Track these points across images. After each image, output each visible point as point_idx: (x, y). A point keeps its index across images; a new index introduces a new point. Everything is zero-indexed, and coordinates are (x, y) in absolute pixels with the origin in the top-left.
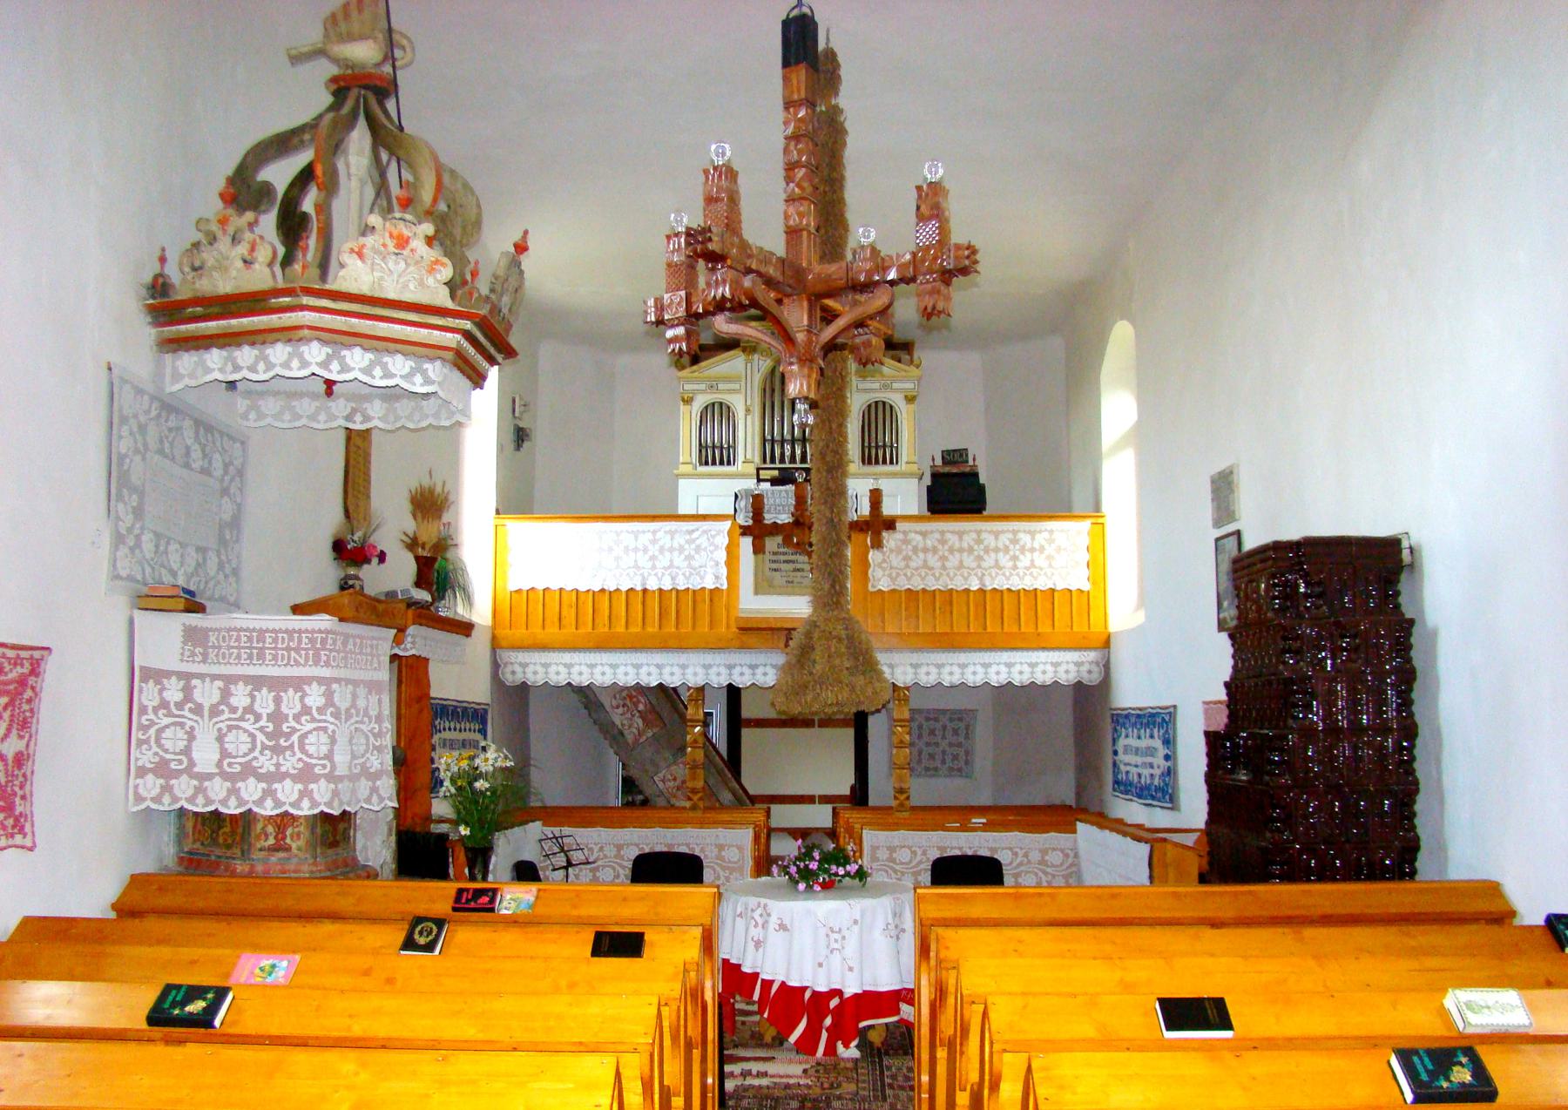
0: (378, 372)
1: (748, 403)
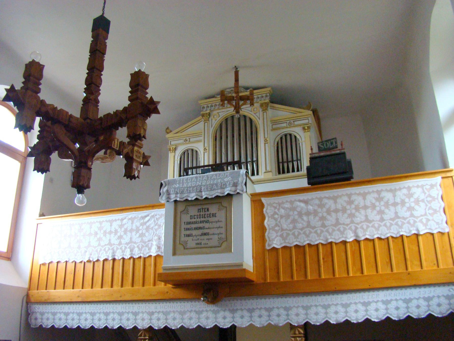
1: (206, 145)
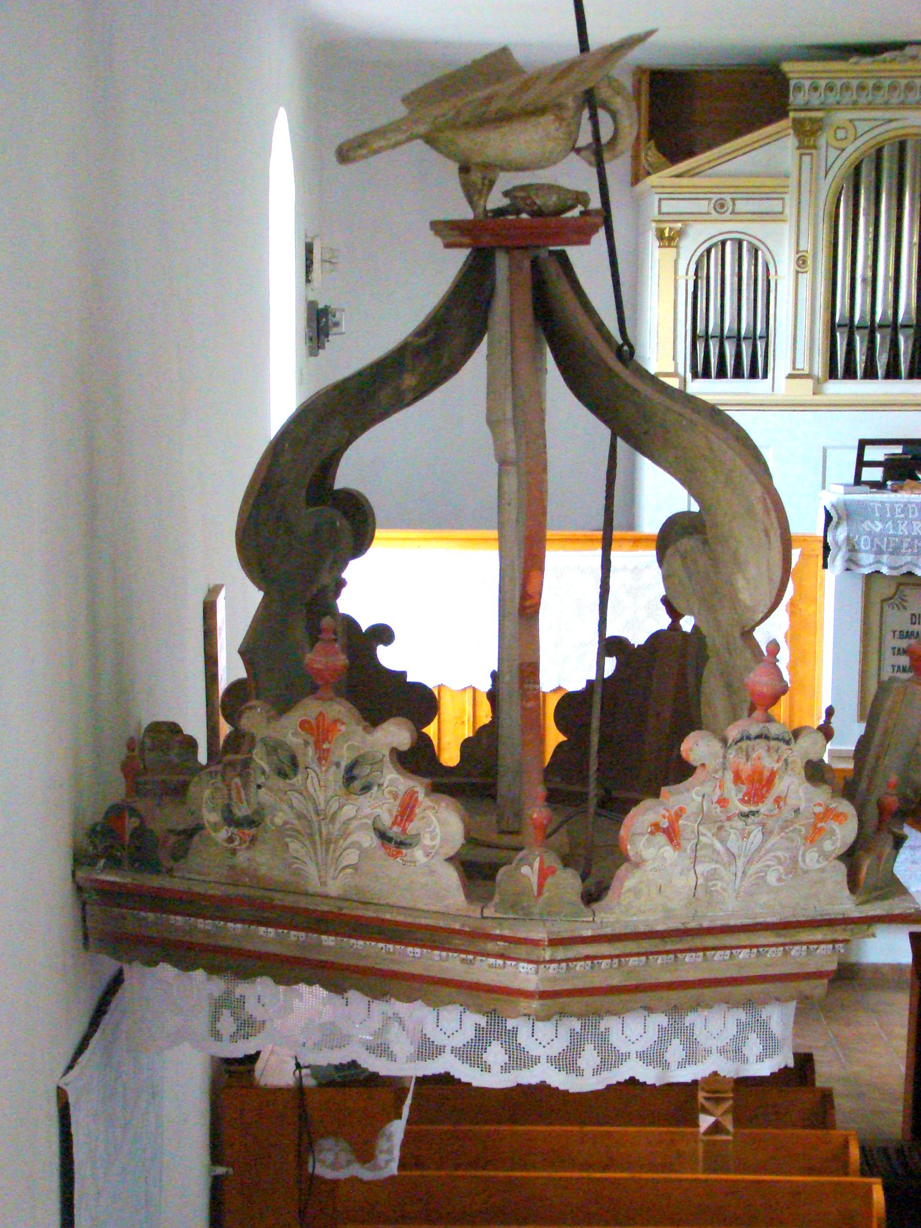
0: (675, 1051)
